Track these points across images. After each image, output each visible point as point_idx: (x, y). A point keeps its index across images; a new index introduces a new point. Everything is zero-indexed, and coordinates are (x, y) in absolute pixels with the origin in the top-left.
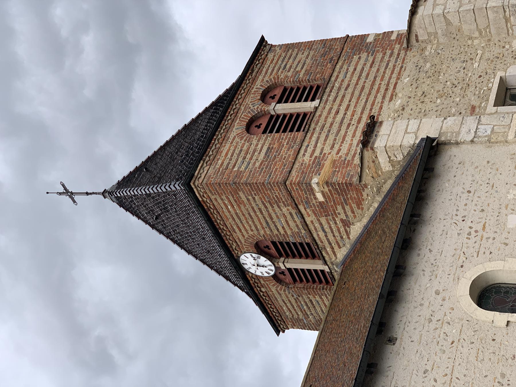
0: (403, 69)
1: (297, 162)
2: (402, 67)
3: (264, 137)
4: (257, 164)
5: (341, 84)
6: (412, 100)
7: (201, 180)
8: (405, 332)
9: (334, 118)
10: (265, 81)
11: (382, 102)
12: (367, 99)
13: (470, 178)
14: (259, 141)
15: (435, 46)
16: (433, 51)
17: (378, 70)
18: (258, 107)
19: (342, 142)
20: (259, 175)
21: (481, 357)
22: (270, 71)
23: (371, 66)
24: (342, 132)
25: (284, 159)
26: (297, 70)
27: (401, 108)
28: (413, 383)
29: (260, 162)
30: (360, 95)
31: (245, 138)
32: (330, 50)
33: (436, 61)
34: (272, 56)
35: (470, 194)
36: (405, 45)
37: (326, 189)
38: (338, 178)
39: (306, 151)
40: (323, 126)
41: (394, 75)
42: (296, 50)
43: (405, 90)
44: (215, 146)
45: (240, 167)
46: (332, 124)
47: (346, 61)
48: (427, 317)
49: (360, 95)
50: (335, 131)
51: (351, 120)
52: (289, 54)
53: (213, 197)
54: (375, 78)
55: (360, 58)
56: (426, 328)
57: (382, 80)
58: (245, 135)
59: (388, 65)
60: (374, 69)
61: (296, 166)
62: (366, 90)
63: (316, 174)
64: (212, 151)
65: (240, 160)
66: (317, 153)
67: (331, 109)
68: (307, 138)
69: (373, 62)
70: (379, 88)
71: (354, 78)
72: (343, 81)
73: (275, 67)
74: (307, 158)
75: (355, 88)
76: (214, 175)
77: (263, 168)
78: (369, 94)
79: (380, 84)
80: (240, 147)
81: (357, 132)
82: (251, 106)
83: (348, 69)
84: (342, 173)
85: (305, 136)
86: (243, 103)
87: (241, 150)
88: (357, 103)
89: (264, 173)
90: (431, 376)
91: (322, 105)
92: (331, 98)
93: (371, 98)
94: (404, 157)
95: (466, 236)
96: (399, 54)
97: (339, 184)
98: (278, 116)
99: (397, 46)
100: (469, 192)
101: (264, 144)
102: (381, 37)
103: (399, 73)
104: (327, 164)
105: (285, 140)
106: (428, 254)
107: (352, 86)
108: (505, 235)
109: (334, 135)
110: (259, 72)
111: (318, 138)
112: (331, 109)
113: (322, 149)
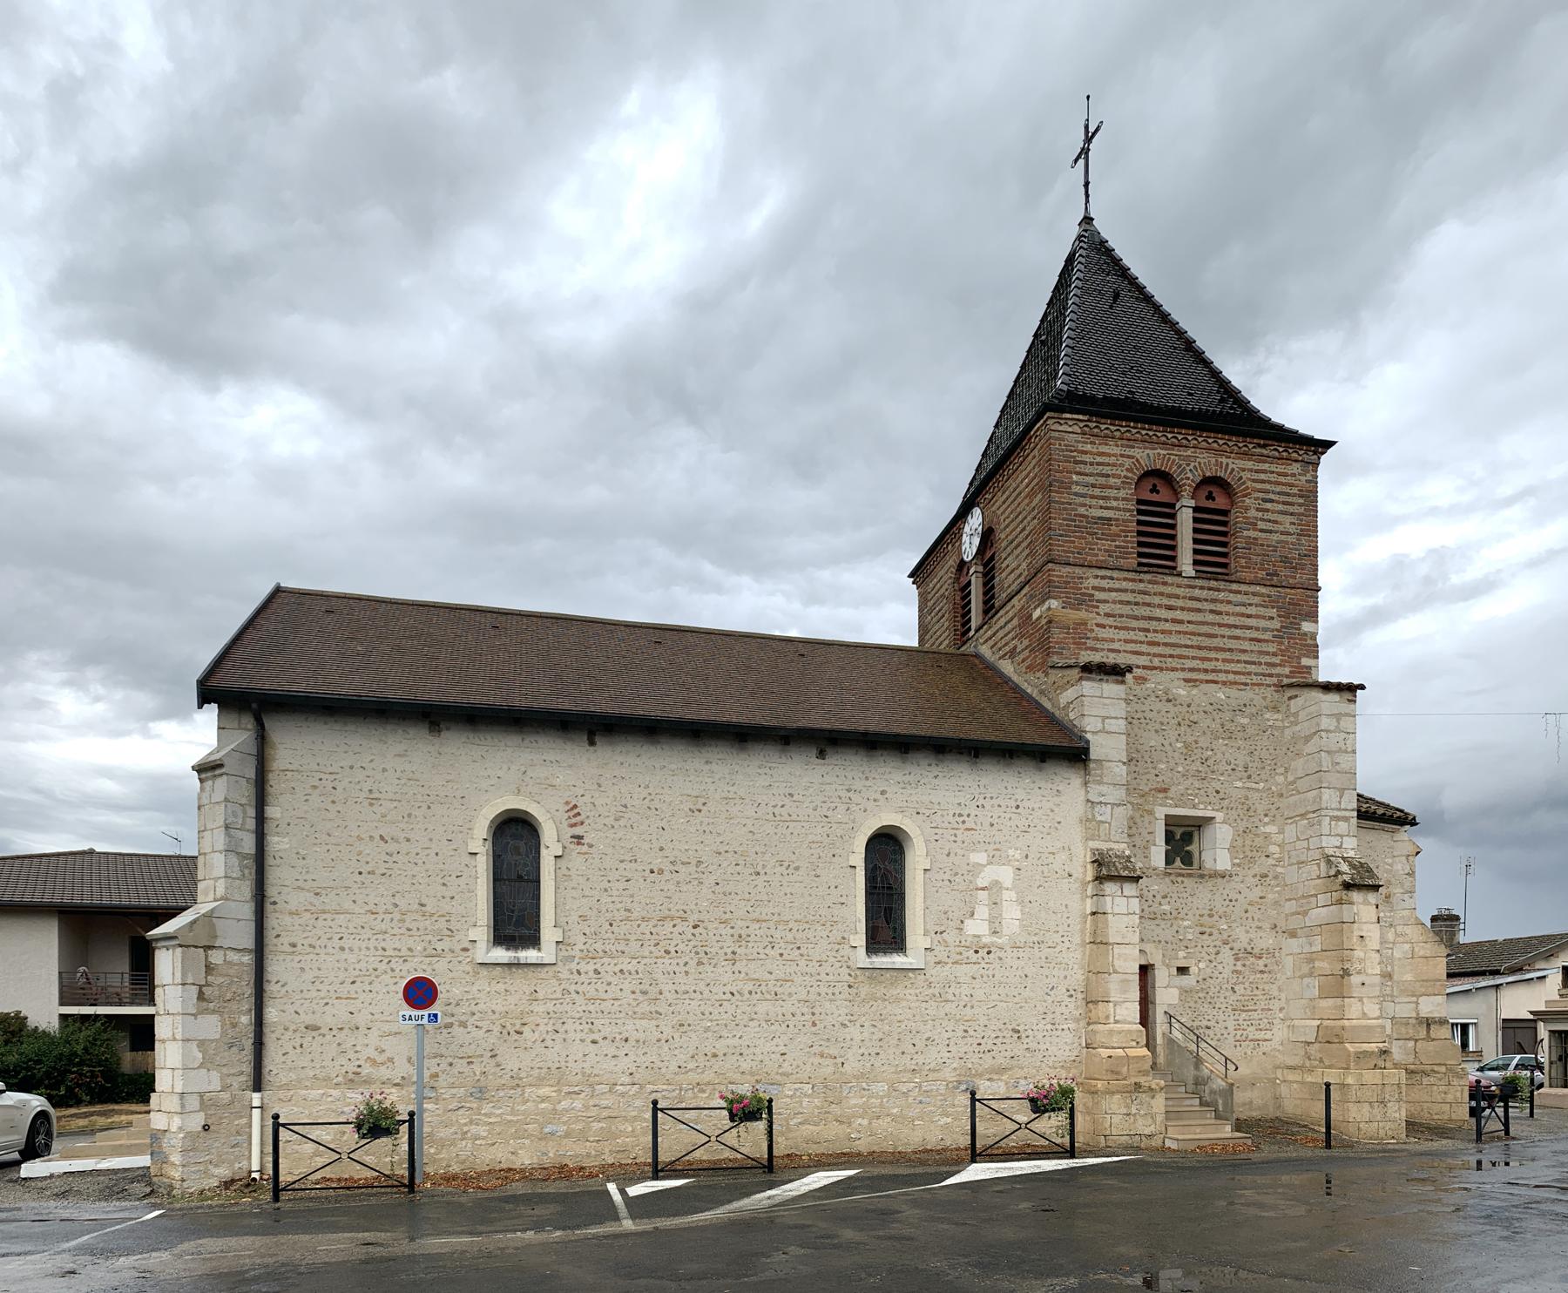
0: (1243, 687)
1: (1084, 569)
2: (1246, 684)
3: (1132, 506)
4: (1082, 510)
5: (1222, 602)
6: (1185, 709)
7: (1056, 427)
8: (831, 767)
9: (1160, 606)
10: (1242, 474)
11: (1183, 670)
12: (1192, 647)
13: (1036, 806)
14: (1123, 499)
15: (1279, 724)
16: (1270, 723)
17: (1244, 651)
18: (1188, 478)
19: (1116, 628)
20: (1064, 519)
21: (814, 846)
22: (1263, 476)
23: (1252, 640)
24: (1135, 624)
25: (1090, 549)
26: (1259, 523)
27: (1171, 697)
28: (777, 784)
29: (1086, 513)
30: (1199, 635)
31: (1130, 475)
32: (1293, 568)
33: (1250, 731)
34: (1295, 471)
35: (1014, 810)
36: (1286, 681)
37: (1044, 621)
38: (1057, 634)
39: (1103, 578)
40: (1145, 593)
41: (1231, 677)
42: (1302, 510)
43: (1204, 698)
44: (1118, 430)
45: (1077, 483)
46: (1149, 605)
47: (1267, 599)
48: (852, 787)
49: (1199, 635)
50: (1136, 613)
51: (1155, 631)
52: (1295, 500)
53: (1036, 451)
54: (1230, 650)
55: (1273, 618)
56: (841, 787)
57: (1224, 660)
58: (1135, 474)
59: (1254, 663)
60: (1246, 645)
61: (1078, 570)
62: (1207, 642)
63: (1063, 602)
64: (1107, 429)
65: (1091, 480)
66: (1099, 595)
67: (1177, 597)
68: (1126, 575)
69: (1259, 641)
70: (1210, 660)
71: (1232, 618)
72: (1229, 602)
73: (1270, 482)
74: (1093, 582)
75: (1213, 624)
76: (1065, 445)
77: (1075, 521)
78: (1200, 648)
79: (1217, 660)
80: (1114, 472)
81: (1133, 645)
82: (1191, 467)
83: (1250, 605)
84: (1065, 638)
85: (1129, 571)
86: (1198, 451)
87: (1108, 476)
88: (1186, 633)
89: (1067, 525)
90: (787, 801)
91: (1186, 581)
92: (1197, 593)
93: (1192, 653)
94: (1071, 721)
95: (957, 813)
96: (1271, 675)
97: (1049, 638)
98: (1173, 516)
99: (1287, 670)
100: (1018, 807)
101: (1118, 509)
102: (1309, 642)
103: (1236, 683)
104: (1083, 614)
105: (1123, 541)
106: (931, 775)
107: (1217, 619)
108: (960, 852)
109: (1131, 613)
110: (1263, 458)
111: (1125, 591)
112: (1177, 597)
113: (1105, 601)
